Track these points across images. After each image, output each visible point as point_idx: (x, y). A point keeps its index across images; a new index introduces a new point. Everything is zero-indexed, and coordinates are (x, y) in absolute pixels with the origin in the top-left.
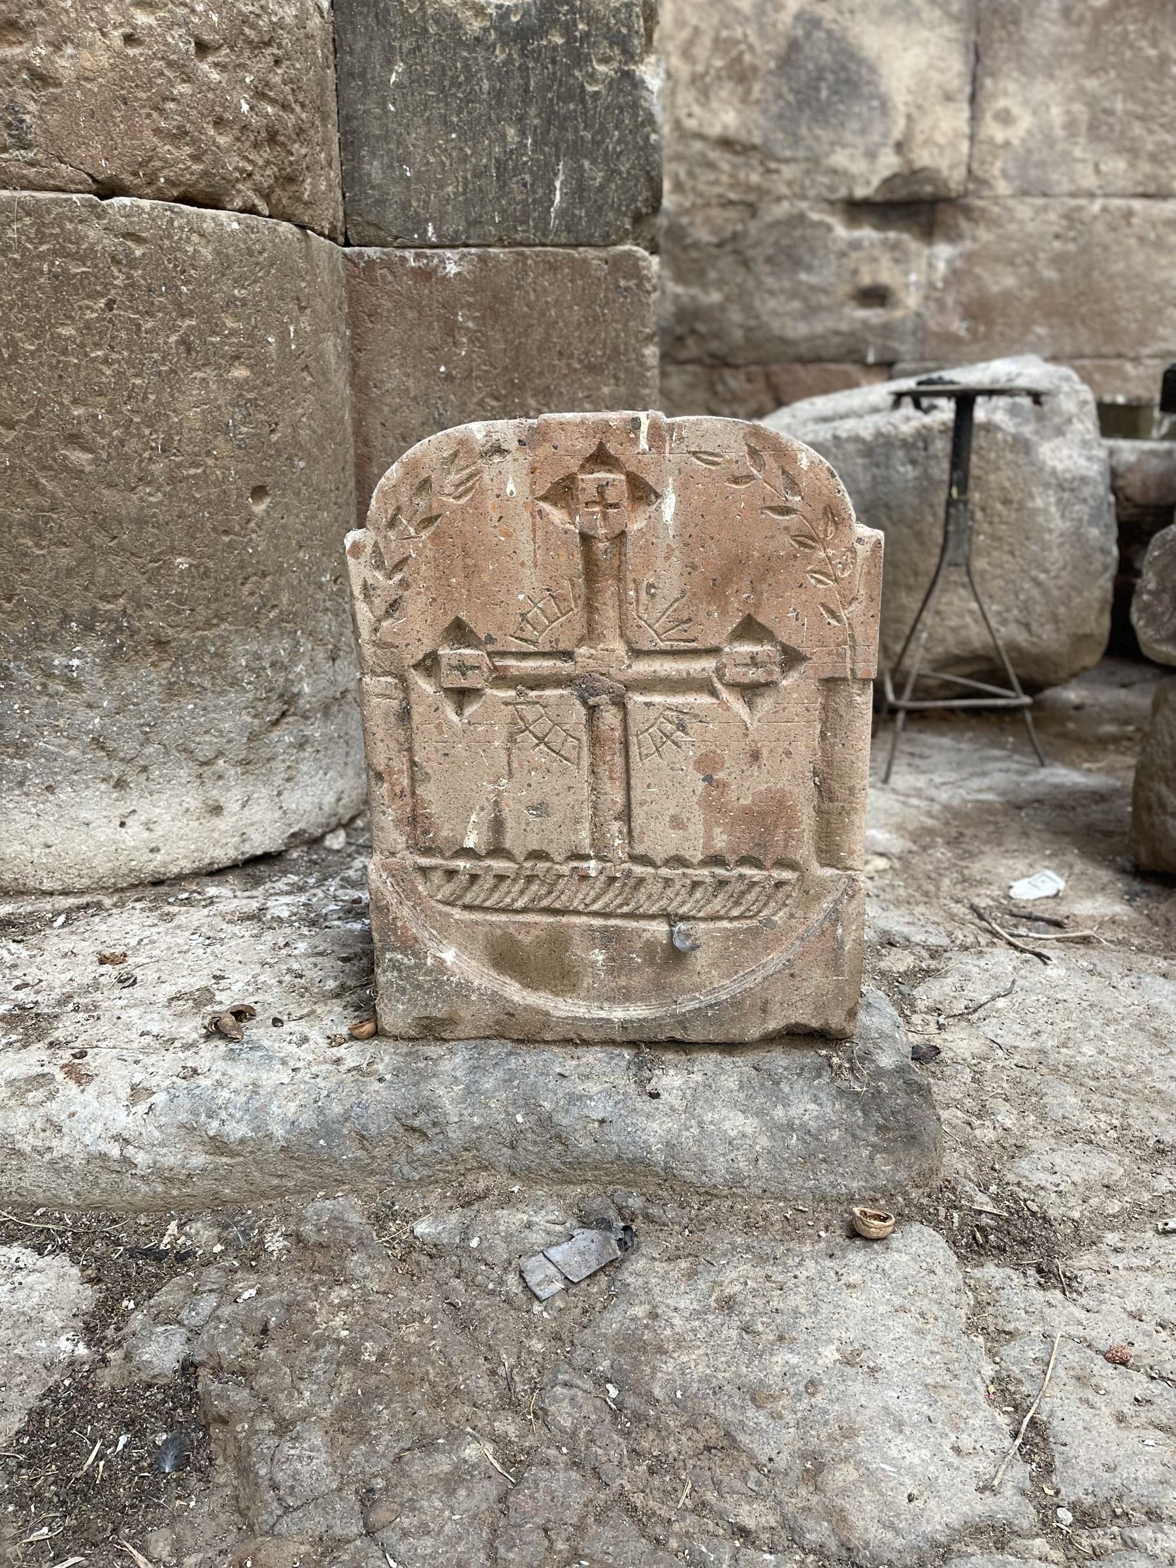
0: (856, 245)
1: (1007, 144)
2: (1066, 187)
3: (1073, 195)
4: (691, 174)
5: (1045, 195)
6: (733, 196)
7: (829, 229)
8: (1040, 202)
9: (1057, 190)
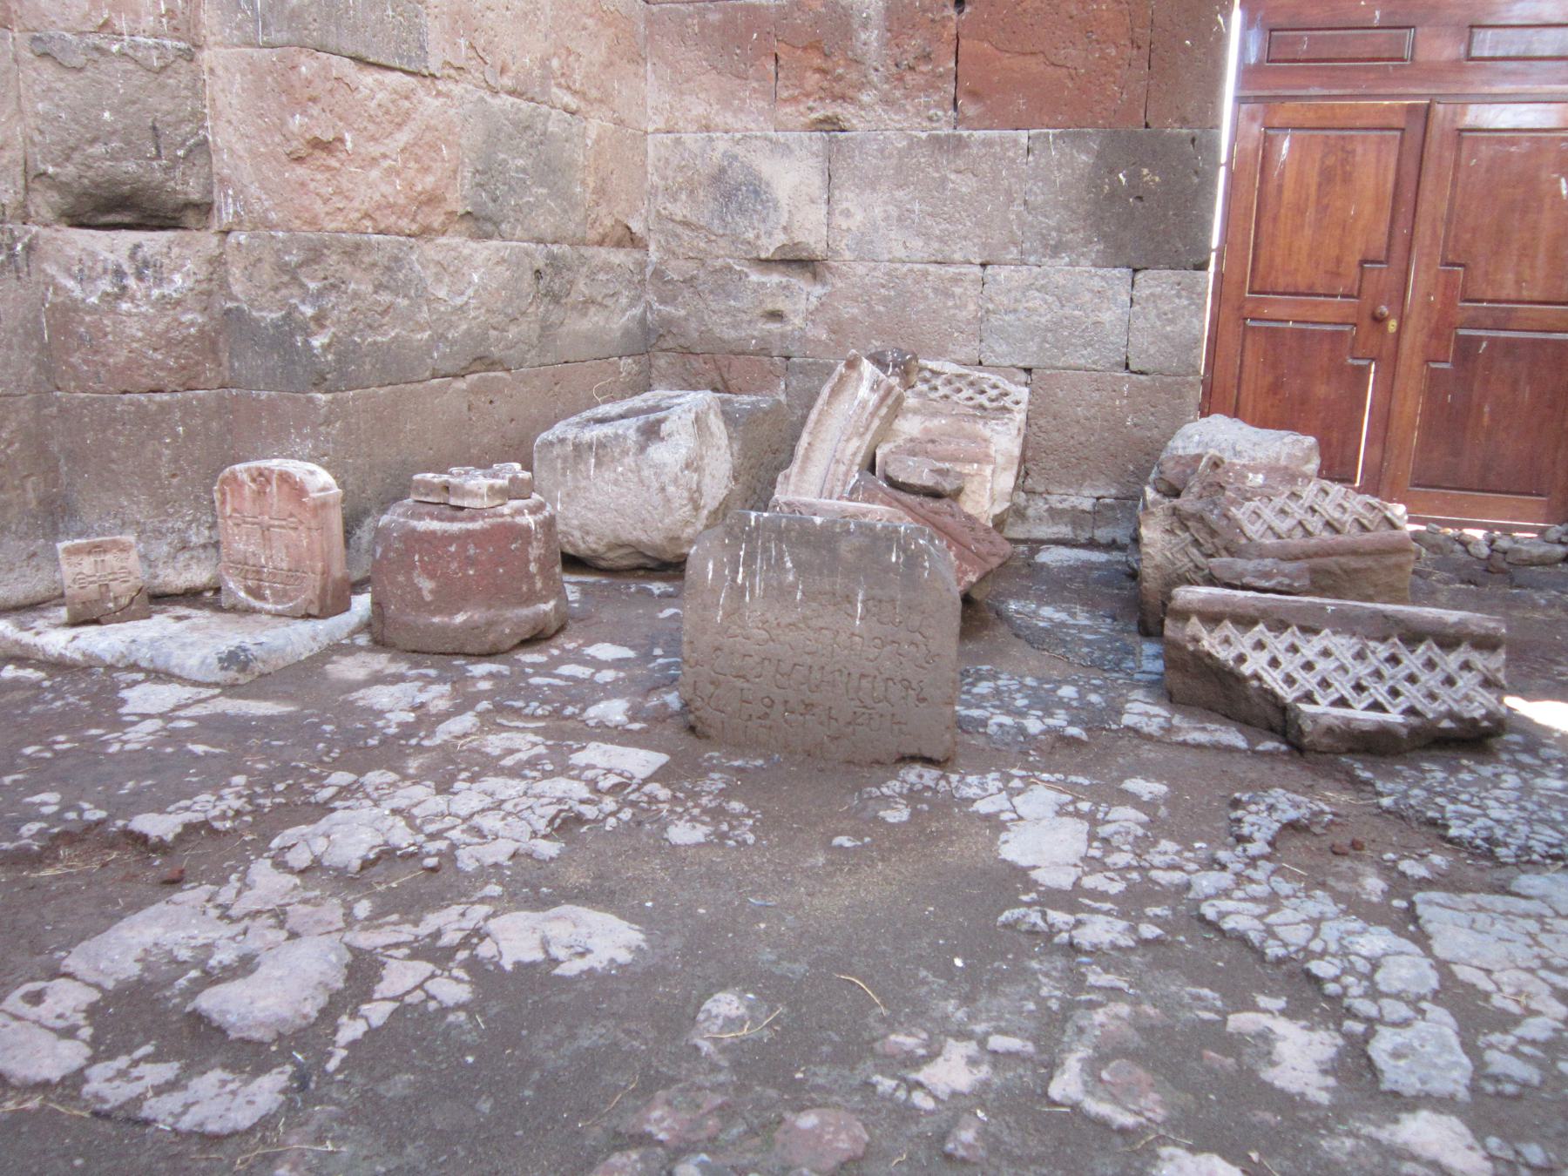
1: (849, 230)
2: (886, 257)
4: (668, 242)
8: (872, 264)
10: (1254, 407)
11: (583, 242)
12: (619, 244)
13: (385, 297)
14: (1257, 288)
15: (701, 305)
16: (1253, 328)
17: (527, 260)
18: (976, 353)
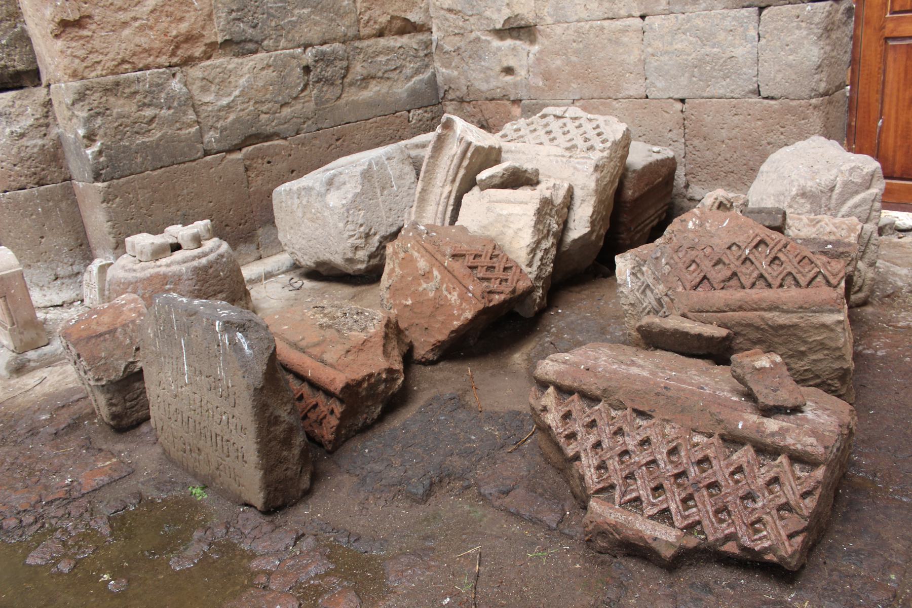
0: (499, 49)
2: (576, 18)
3: (578, 21)
5: (567, 22)
6: (456, 31)
7: (489, 42)
8: (566, 25)
9: (571, 20)
10: (897, 119)
11: (358, 38)
12: (401, 32)
13: (148, 112)
14: (897, 9)
15: (466, 67)
16: (894, 46)
17: (294, 62)
18: (643, 89)
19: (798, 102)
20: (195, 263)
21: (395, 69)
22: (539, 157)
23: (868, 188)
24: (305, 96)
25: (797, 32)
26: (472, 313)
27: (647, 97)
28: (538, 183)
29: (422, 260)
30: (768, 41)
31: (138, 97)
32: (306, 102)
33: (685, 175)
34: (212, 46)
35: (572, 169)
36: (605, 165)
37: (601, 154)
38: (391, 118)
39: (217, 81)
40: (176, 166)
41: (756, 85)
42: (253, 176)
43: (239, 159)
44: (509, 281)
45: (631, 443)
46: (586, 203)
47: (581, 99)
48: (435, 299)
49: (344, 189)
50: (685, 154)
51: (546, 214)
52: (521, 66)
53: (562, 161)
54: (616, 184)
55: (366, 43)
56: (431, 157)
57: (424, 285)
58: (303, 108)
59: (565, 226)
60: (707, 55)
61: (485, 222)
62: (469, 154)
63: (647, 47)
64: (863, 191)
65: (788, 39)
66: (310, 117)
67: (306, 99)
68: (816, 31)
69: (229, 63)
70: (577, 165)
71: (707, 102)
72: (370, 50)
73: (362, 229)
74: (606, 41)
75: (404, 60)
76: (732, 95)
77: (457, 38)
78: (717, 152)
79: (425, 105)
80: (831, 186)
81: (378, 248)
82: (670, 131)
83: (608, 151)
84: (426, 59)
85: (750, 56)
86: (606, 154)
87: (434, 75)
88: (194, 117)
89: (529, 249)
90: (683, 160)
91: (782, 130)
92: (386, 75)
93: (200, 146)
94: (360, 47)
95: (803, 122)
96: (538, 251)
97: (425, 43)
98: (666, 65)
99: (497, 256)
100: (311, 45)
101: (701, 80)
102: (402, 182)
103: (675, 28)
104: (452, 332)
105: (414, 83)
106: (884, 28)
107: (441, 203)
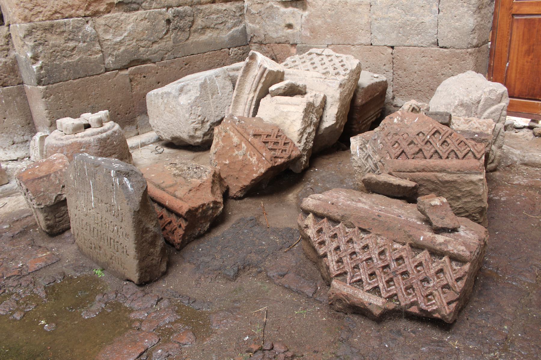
0: (284, 13)
7: (278, 9)
10: (517, 62)
13: (71, 44)
15: (264, 23)
16: (517, 19)
19: (461, 50)
20: (99, 136)
21: (222, 23)
22: (307, 78)
23: (499, 102)
24: (167, 37)
25: (461, 9)
26: (265, 169)
27: (371, 45)
28: (305, 93)
29: (236, 137)
30: (444, 13)
31: (65, 35)
32: (168, 41)
33: (393, 92)
34: (111, 5)
35: (326, 85)
36: (345, 84)
37: (343, 77)
38: (218, 53)
39: (114, 26)
40: (88, 77)
41: (436, 40)
42: (135, 84)
43: (126, 75)
44: (287, 151)
45: (357, 248)
46: (334, 106)
47: (332, 44)
48: (243, 160)
49: (189, 94)
50: (393, 79)
51: (310, 112)
52: (297, 23)
53: (320, 81)
54: (352, 96)
55: (203, 7)
56: (242, 76)
57: (237, 152)
58: (166, 44)
59: (321, 119)
60: (408, 21)
61: (274, 116)
62: (265, 75)
63: (373, 15)
64: (497, 104)
65: (456, 13)
66: (169, 50)
67: (168, 40)
68: (472, 8)
69: (121, 16)
70: (329, 84)
71: (407, 48)
72: (207, 11)
73: (200, 118)
74: (348, 10)
75: (227, 17)
76: (422, 45)
77: (259, 6)
78: (412, 78)
79: (240, 45)
80: (478, 100)
81: (209, 130)
82: (385, 65)
83: (348, 76)
84: (241, 18)
85: (433, 22)
86: (346, 77)
87: (245, 27)
88: (99, 48)
89: (299, 133)
90: (392, 82)
91: (450, 66)
92: (216, 27)
93: (102, 65)
94: (201, 9)
95: (463, 62)
96: (304, 134)
97: (240, 8)
98: (383, 26)
99: (280, 136)
100: (171, 7)
101: (404, 36)
102: (225, 90)
103: (390, 4)
104: (253, 180)
105: (233, 32)
106: (512, 8)
107: (248, 103)
